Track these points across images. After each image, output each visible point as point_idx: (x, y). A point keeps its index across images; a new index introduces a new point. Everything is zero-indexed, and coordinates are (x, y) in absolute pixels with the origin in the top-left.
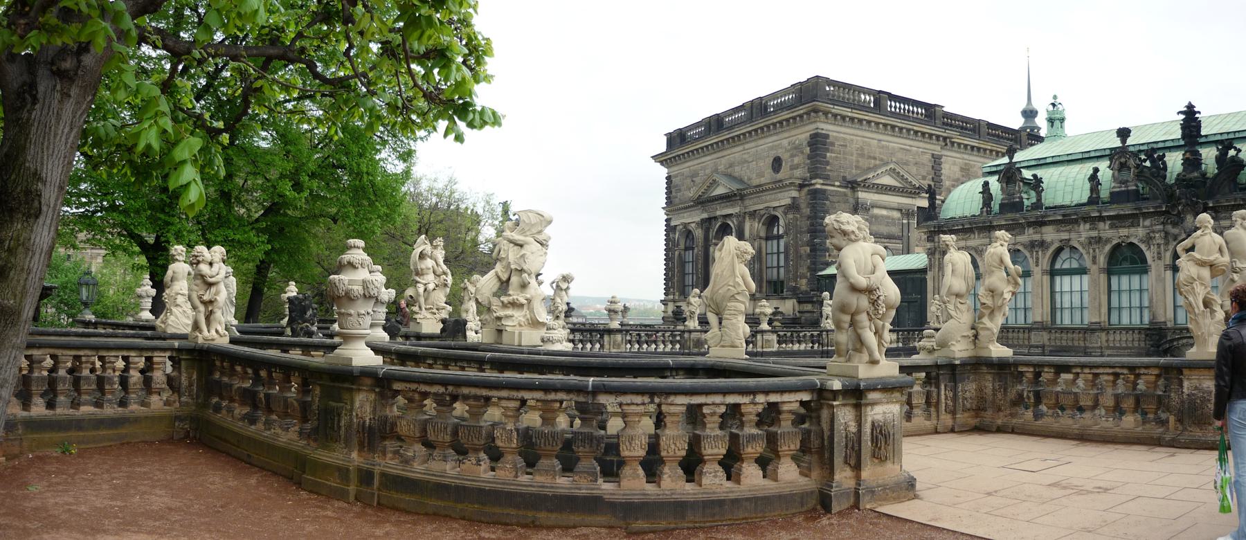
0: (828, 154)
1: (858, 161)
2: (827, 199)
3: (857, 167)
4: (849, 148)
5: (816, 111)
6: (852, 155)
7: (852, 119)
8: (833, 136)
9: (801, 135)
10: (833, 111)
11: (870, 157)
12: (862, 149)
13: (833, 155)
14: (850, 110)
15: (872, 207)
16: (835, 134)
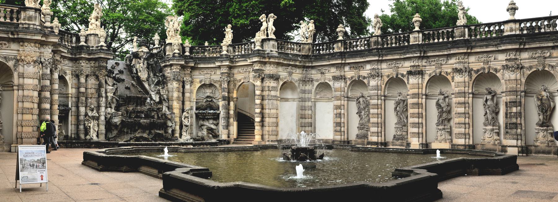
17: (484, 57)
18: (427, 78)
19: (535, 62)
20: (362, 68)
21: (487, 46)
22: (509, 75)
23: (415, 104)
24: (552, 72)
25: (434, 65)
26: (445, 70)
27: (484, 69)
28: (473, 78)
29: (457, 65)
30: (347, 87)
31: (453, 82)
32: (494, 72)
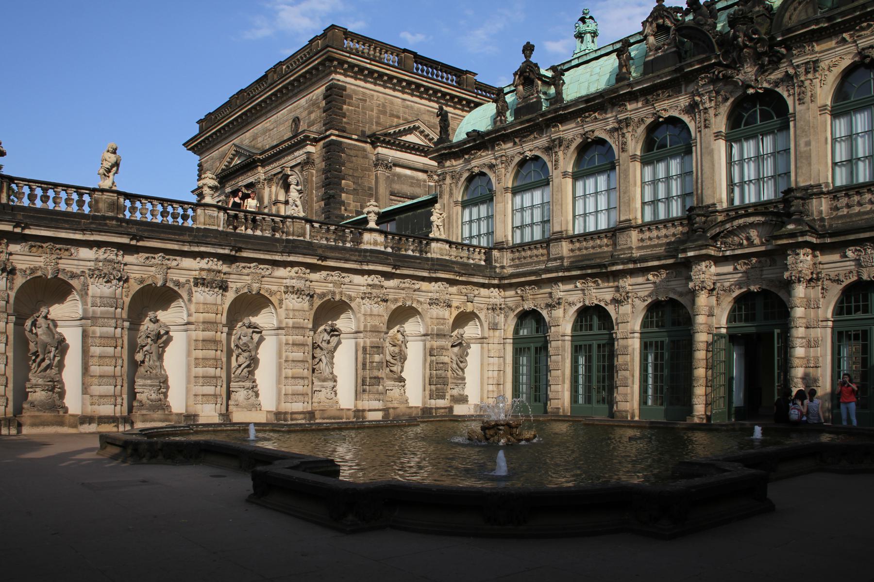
0: (345, 107)
1: (378, 118)
2: (344, 152)
3: (378, 123)
4: (368, 103)
5: (331, 59)
6: (372, 111)
7: (372, 72)
8: (351, 89)
9: (319, 92)
10: (350, 60)
11: (392, 115)
12: (384, 106)
13: (350, 108)
14: (369, 61)
15: (395, 165)
16: (353, 87)
17: (335, 276)
18: (231, 296)
19: (402, 294)
20: (67, 253)
21: (347, 260)
22: (371, 309)
23: (209, 341)
24: (420, 310)
25: (248, 275)
26: (267, 286)
27: (334, 293)
28: (316, 306)
29: (294, 281)
30: (15, 290)
31: (281, 308)
32: (347, 301)
